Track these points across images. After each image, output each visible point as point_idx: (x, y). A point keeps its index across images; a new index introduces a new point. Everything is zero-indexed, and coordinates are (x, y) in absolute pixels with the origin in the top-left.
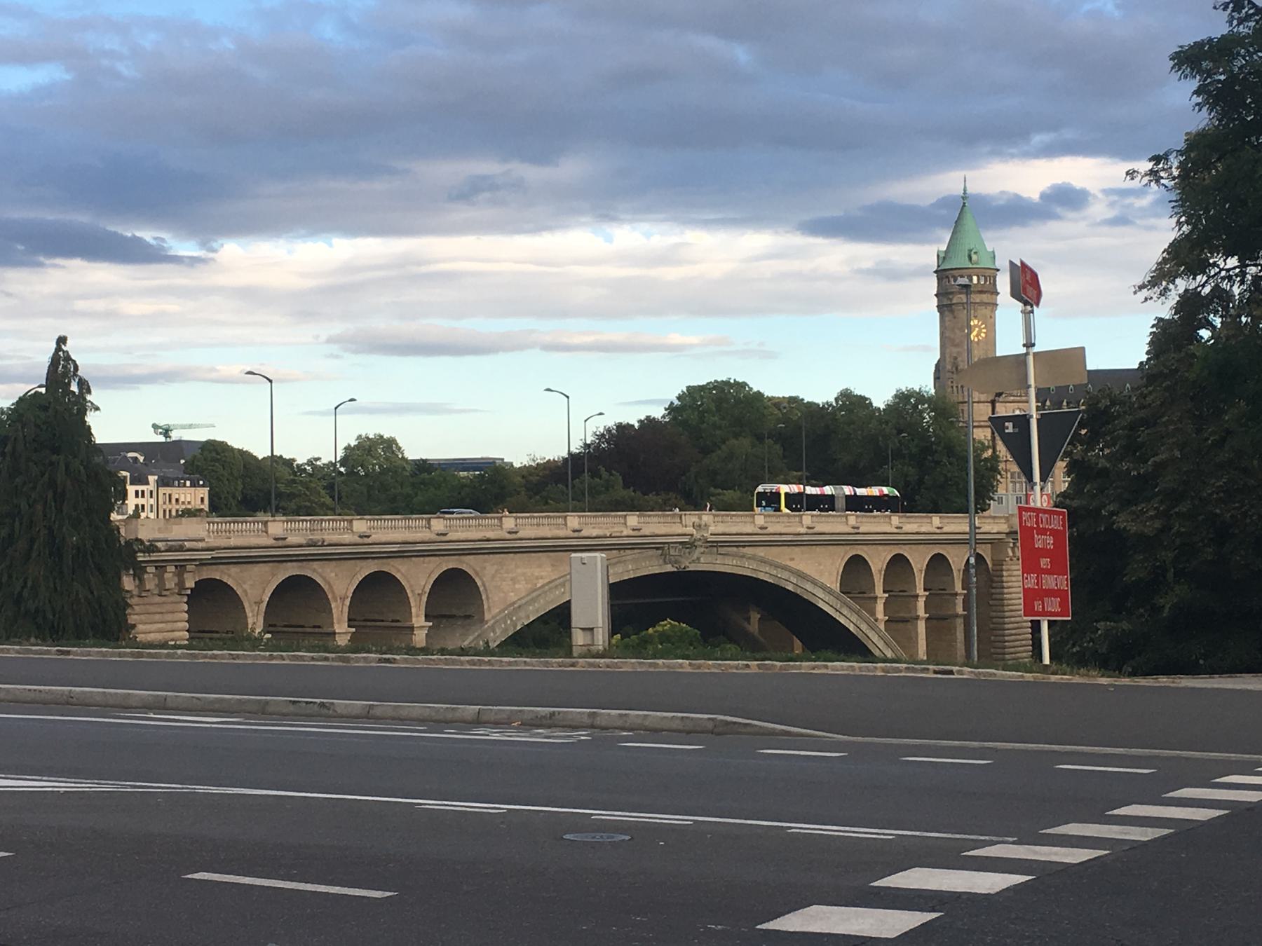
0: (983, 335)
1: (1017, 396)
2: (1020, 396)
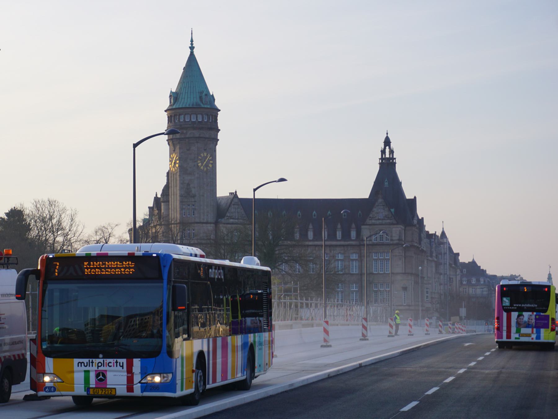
0: (210, 166)
1: (235, 219)
2: (238, 219)
